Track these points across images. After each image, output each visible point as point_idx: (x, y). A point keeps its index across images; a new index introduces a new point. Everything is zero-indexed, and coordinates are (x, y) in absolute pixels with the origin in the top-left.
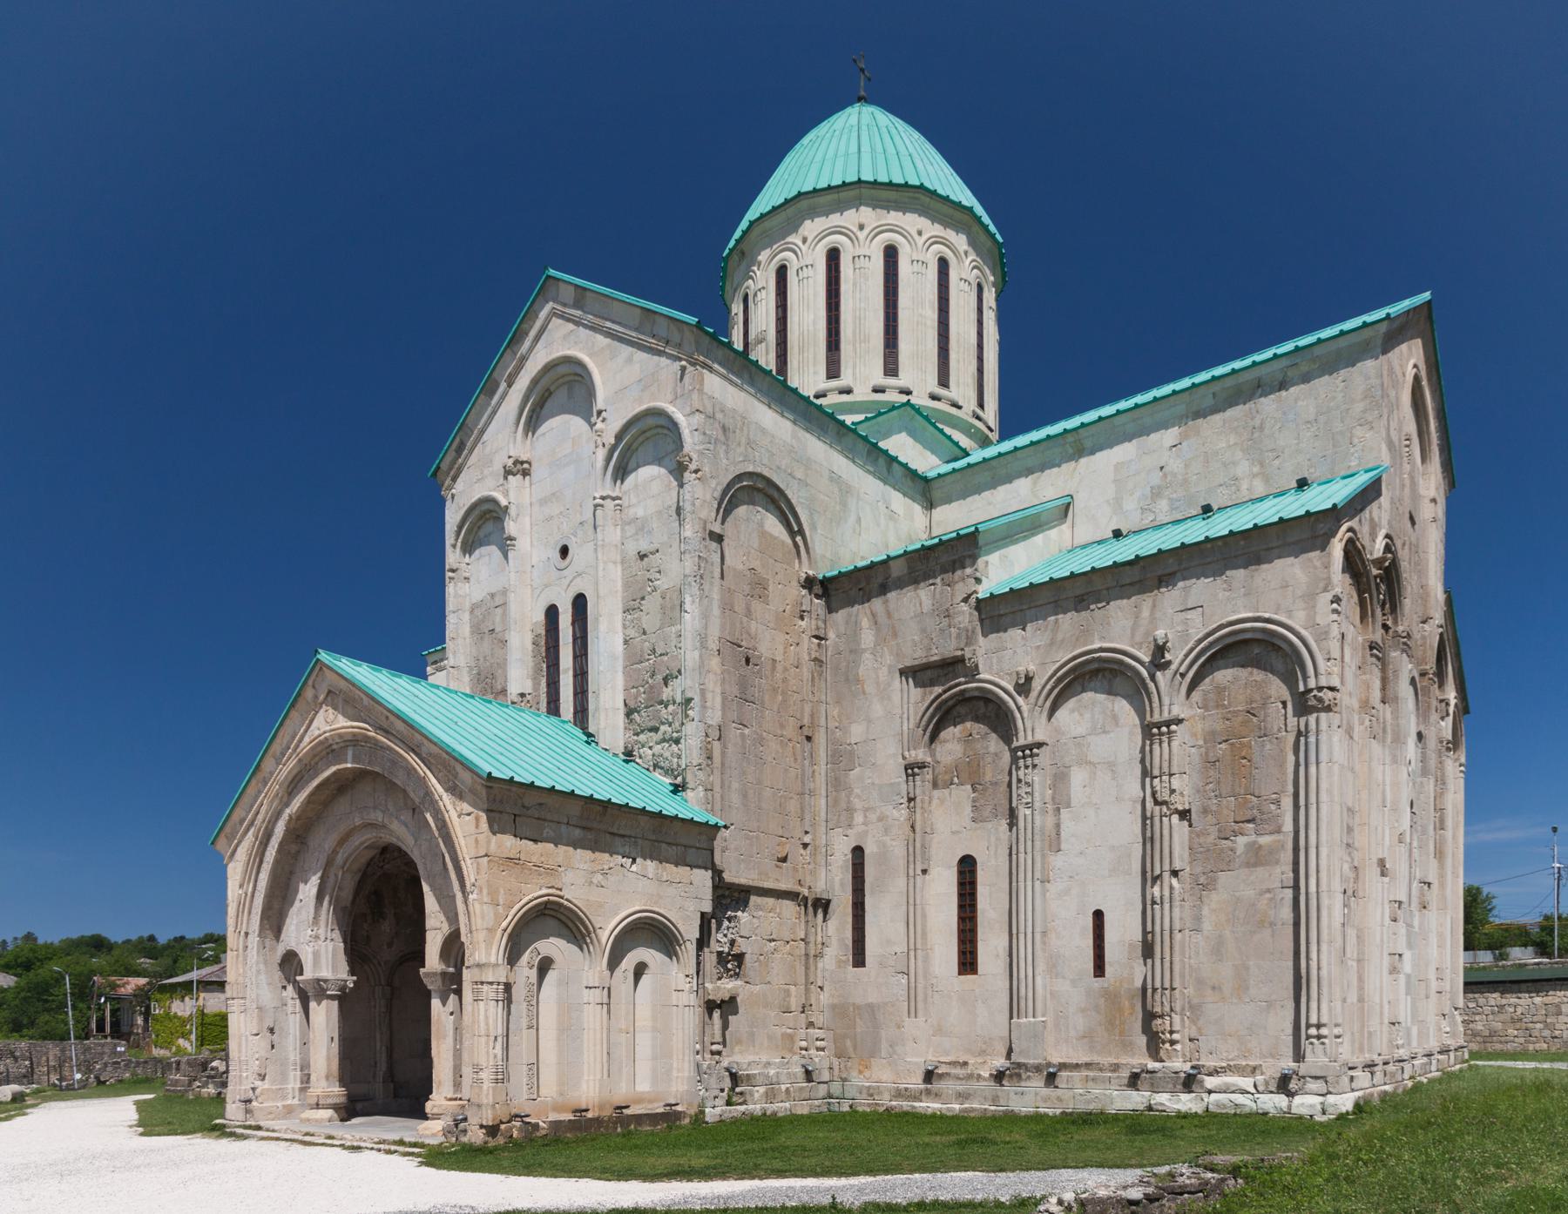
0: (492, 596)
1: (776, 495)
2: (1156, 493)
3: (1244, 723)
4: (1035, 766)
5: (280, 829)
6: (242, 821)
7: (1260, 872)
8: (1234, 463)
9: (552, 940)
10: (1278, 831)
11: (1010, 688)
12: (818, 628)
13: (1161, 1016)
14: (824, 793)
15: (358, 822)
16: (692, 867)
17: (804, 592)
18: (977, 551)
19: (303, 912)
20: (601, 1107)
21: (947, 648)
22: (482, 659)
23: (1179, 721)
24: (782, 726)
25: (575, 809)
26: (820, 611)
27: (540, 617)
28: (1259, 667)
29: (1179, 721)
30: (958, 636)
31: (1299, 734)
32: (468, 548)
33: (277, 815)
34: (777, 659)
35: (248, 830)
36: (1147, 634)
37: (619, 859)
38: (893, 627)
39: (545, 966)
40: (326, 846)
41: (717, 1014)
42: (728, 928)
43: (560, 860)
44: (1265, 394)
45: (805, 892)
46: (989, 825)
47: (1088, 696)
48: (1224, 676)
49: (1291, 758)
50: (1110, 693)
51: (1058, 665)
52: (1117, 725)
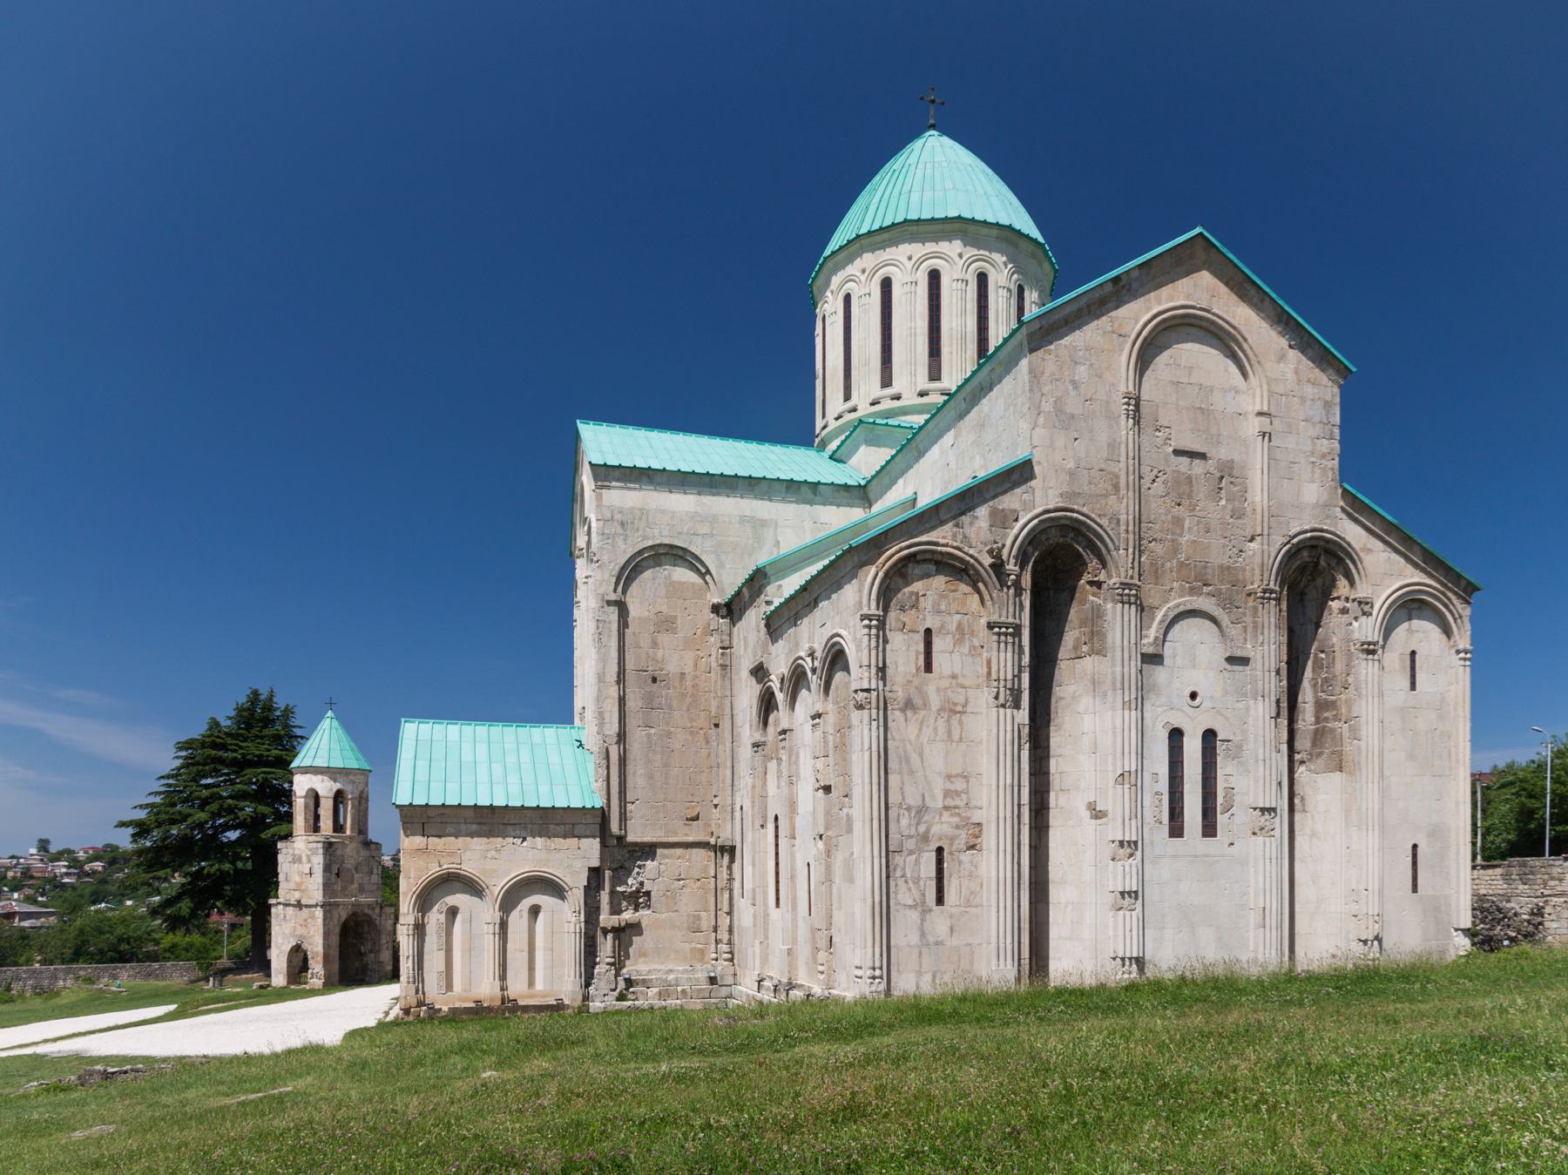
1: (680, 553)
9: (458, 895)
12: (722, 642)
14: (729, 764)
16: (579, 837)
17: (712, 615)
18: (765, 581)
20: (492, 999)
24: (691, 720)
25: (471, 814)
26: (724, 628)
34: (687, 672)
37: (511, 840)
39: (453, 912)
41: (610, 936)
42: (638, 874)
43: (460, 846)
44: (985, 397)
45: (713, 841)
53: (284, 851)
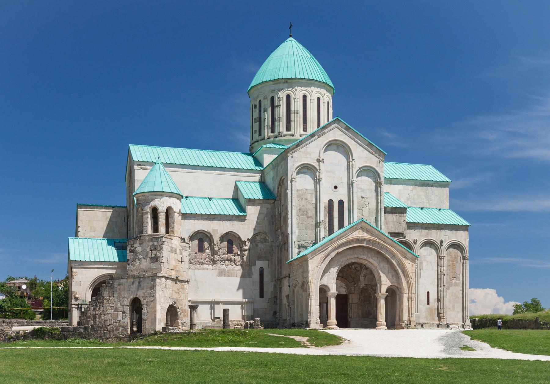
0: (307, 190)
2: (408, 199)
3: (454, 259)
4: (418, 260)
5: (333, 255)
6: (319, 251)
7: (456, 287)
8: (423, 199)
10: (459, 280)
11: (412, 242)
13: (442, 313)
15: (356, 256)
21: (400, 231)
22: (302, 206)
23: (445, 257)
27: (327, 202)
28: (456, 249)
29: (445, 257)
30: (402, 228)
31: (463, 263)
32: (298, 173)
33: (333, 251)
35: (320, 253)
36: (439, 238)
38: (386, 222)
40: (341, 260)
47: (426, 247)
48: (451, 250)
49: (462, 267)
50: (431, 247)
51: (422, 240)
52: (432, 254)
53: (166, 243)
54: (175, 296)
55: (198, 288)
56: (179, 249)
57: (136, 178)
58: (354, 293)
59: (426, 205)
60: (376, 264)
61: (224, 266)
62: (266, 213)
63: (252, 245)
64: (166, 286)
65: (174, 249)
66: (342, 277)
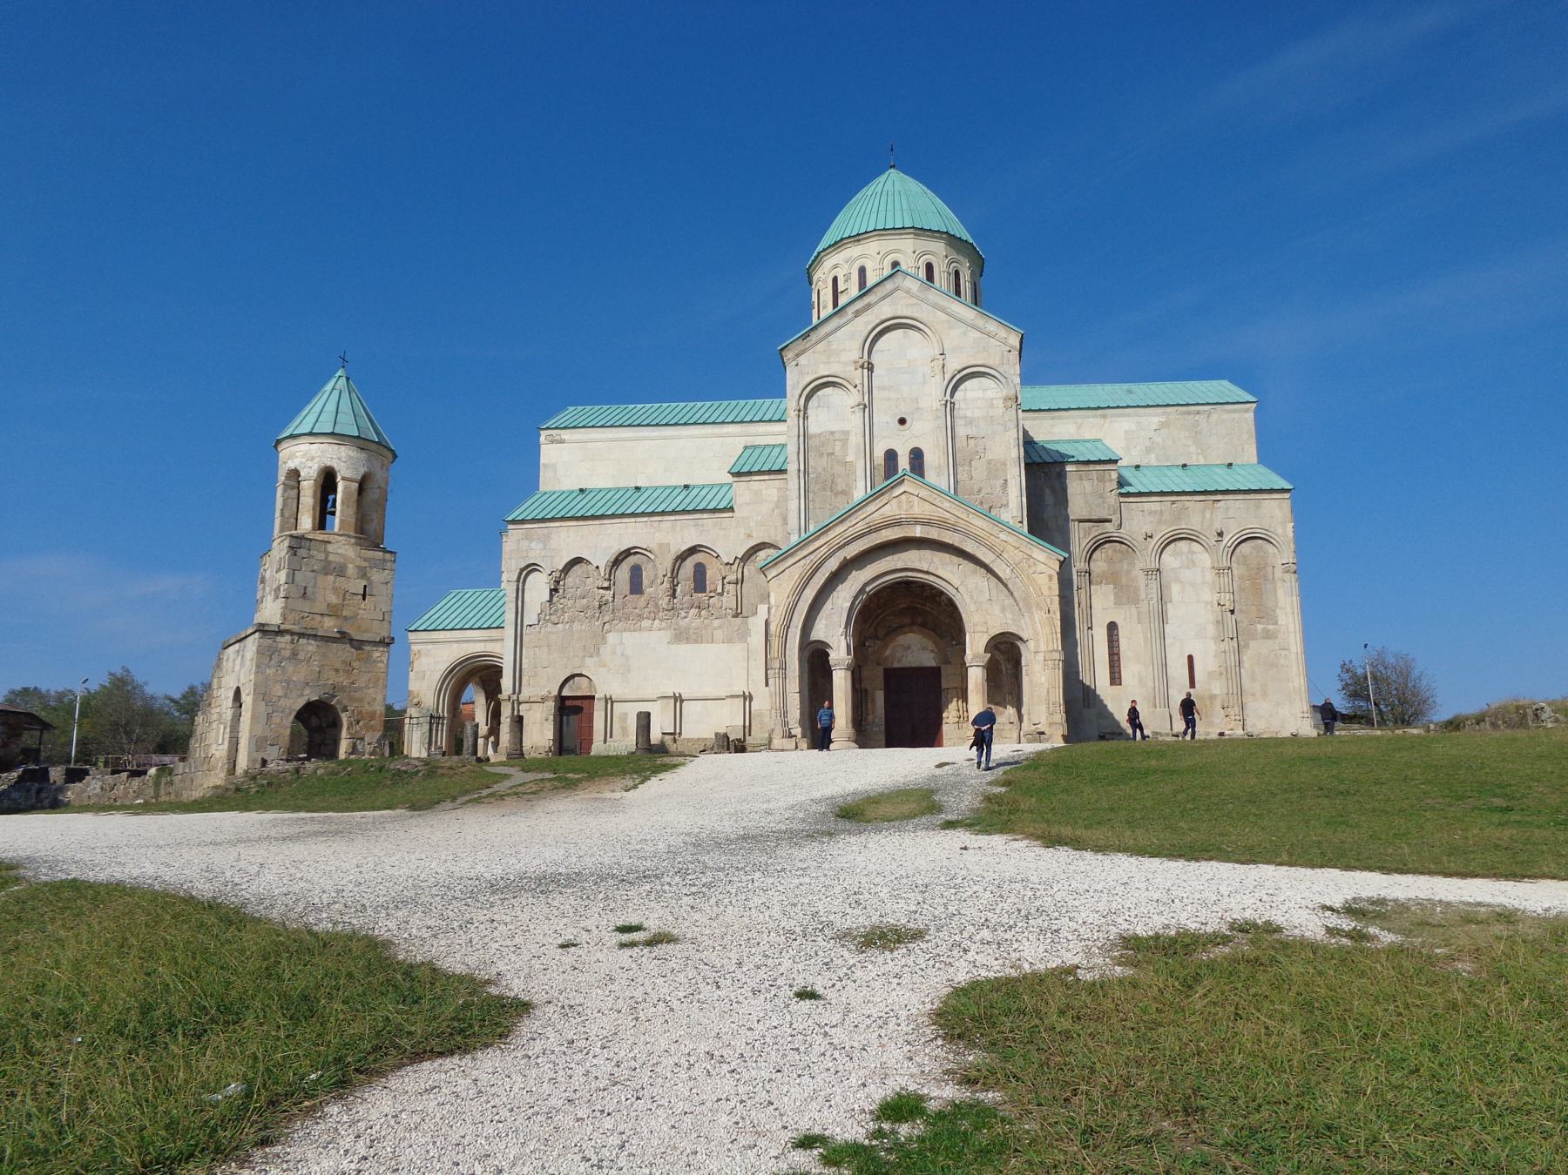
2: (1148, 451)
5: (833, 564)
8: (1189, 446)
19: (835, 617)
22: (820, 470)
30: (1109, 509)
46: (1125, 607)
54: (331, 678)
55: (629, 671)
56: (358, 567)
57: (542, 461)
58: (949, 663)
59: (1197, 460)
60: (956, 583)
61: (686, 620)
62: (776, 499)
63: (749, 570)
64: (294, 654)
65: (333, 566)
66: (924, 625)
